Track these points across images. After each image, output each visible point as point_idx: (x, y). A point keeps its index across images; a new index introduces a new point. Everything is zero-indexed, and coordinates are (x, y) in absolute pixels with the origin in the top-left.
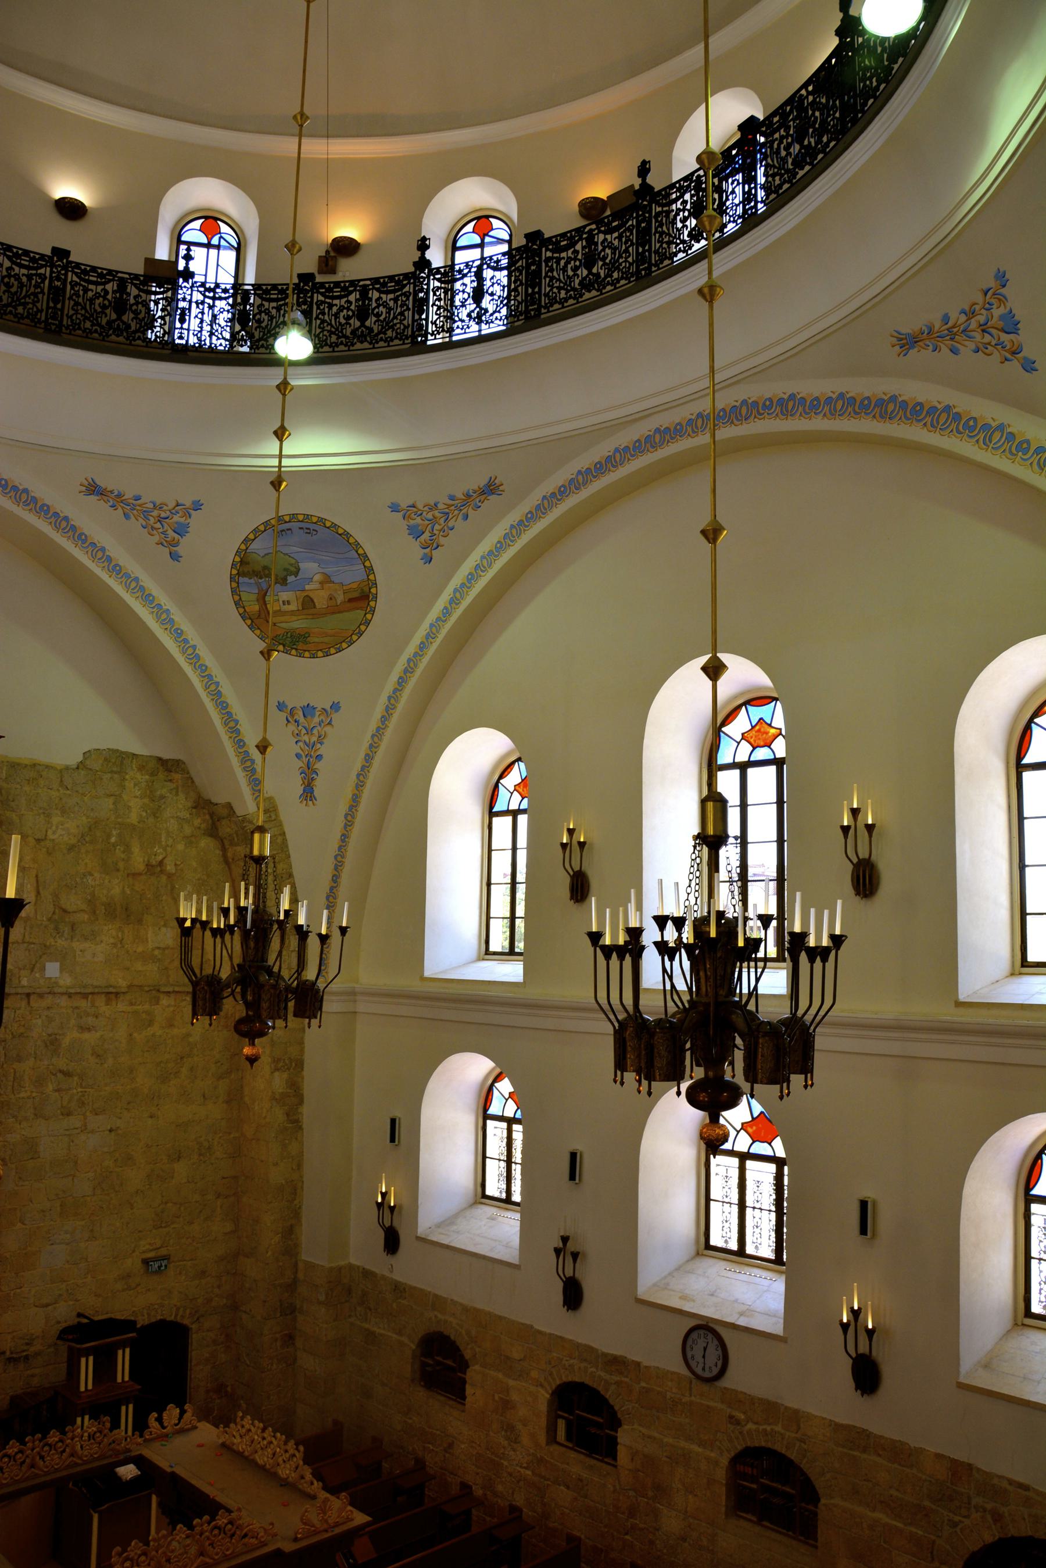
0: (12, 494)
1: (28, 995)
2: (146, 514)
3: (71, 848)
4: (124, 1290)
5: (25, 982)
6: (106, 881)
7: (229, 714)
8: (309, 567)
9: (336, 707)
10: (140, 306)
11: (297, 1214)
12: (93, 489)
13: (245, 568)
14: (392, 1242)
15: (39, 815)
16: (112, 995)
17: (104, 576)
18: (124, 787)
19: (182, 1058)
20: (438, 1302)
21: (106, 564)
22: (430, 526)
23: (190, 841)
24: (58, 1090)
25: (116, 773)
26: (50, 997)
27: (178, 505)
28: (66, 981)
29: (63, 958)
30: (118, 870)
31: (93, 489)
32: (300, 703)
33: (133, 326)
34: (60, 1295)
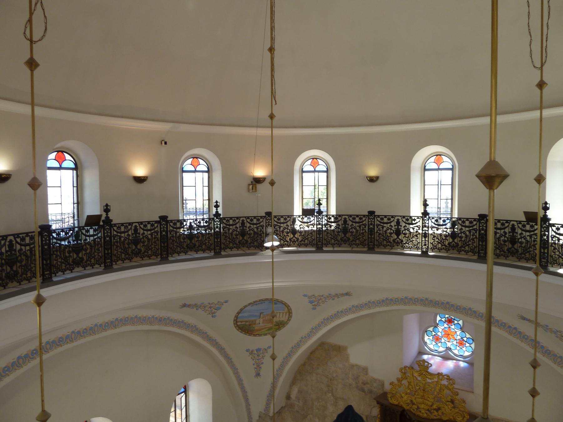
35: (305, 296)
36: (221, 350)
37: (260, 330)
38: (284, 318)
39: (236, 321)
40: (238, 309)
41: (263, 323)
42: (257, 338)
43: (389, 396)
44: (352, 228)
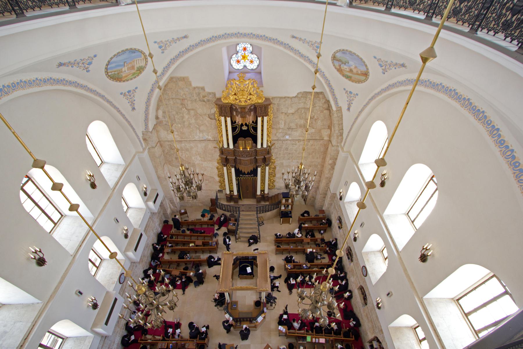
2: (308, 43)
7: (332, 88)
8: (351, 63)
9: (357, 95)
11: (330, 181)
12: (293, 37)
13: (334, 58)
14: (341, 199)
16: (299, 140)
20: (342, 214)
22: (385, 67)
23: (322, 112)
28: (290, 139)
29: (289, 135)
31: (293, 37)
35: (155, 42)
36: (103, 97)
37: (126, 76)
38: (143, 64)
39: (107, 72)
40: (106, 62)
41: (128, 70)
42: (126, 83)
43: (222, 99)
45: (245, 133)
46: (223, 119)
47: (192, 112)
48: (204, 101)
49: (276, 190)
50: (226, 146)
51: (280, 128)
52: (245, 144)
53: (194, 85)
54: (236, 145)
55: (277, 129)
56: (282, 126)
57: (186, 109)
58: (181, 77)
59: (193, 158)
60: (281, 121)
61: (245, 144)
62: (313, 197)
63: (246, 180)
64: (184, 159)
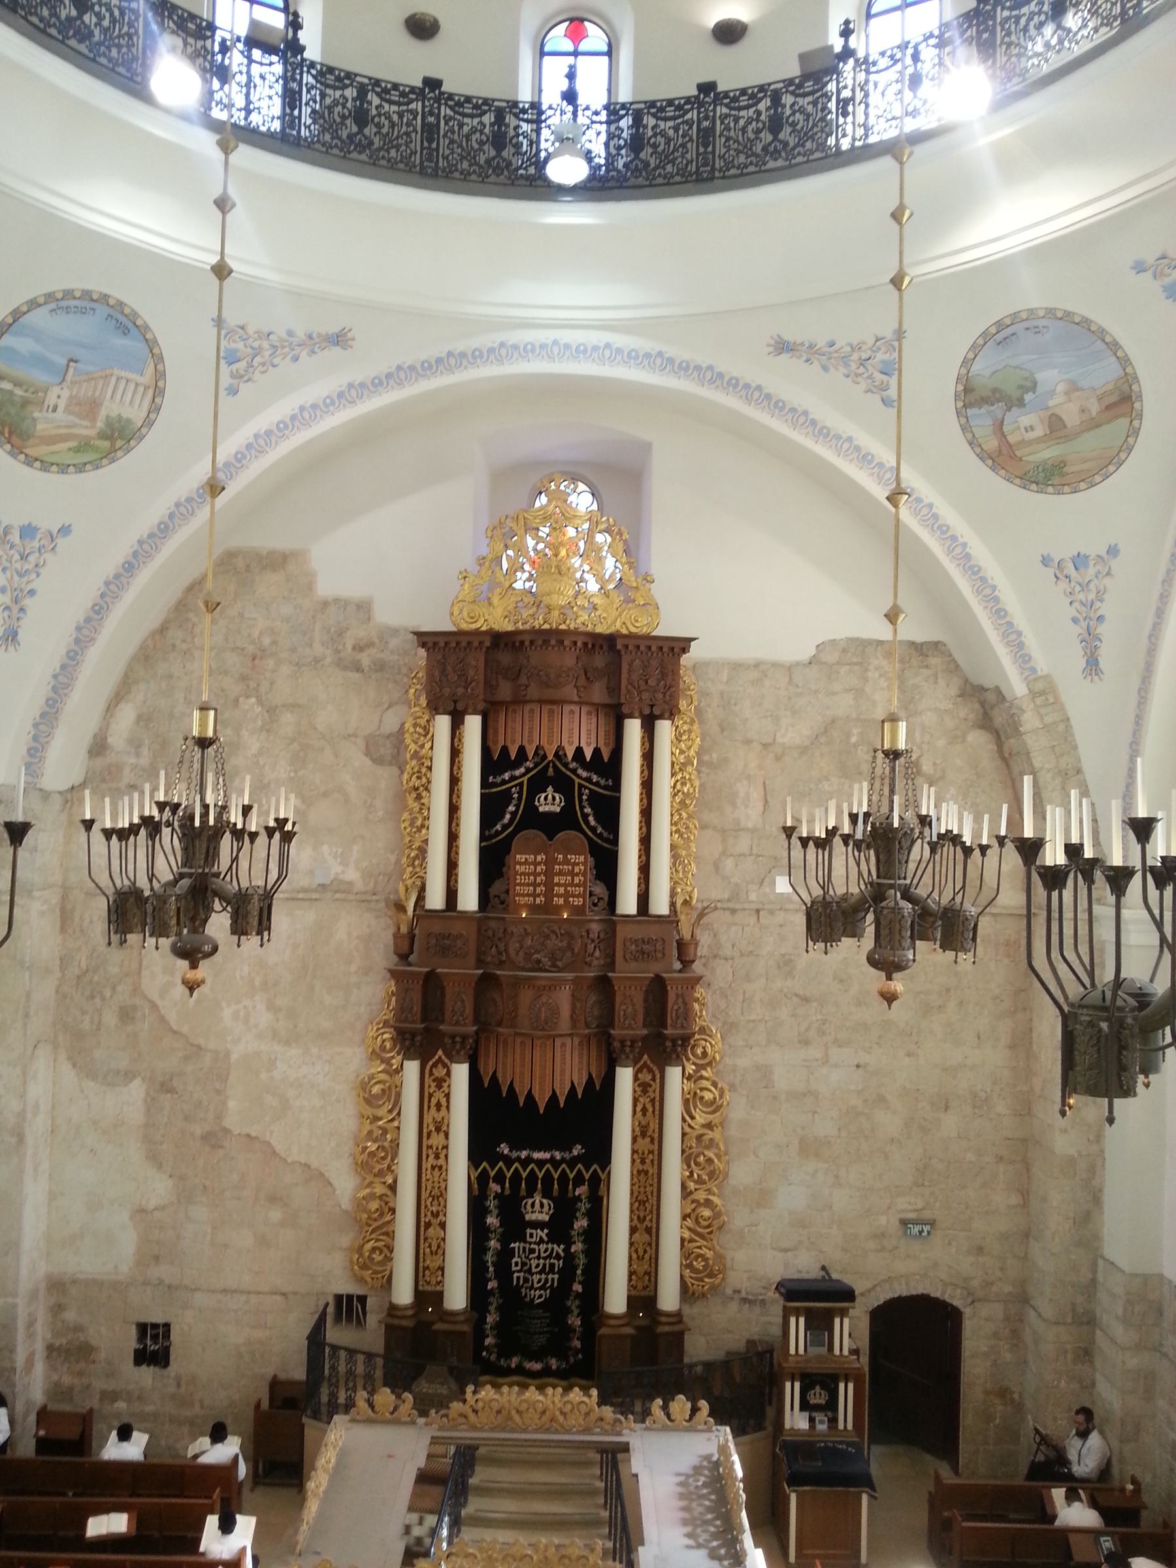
0: (696, 374)
1: (758, 911)
3: (803, 750)
4: (878, 1251)
5: (753, 896)
6: (846, 787)
10: (797, 114)
12: (783, 347)
15: (766, 717)
17: (809, 443)
18: (866, 680)
19: (948, 990)
21: (810, 429)
24: (793, 1015)
25: (856, 664)
26: (782, 914)
27: (877, 340)
30: (860, 773)
31: (783, 347)
32: (1068, 553)
33: (792, 142)
34: (801, 1242)
44: (379, 115)
45: (551, 808)
46: (443, 723)
47: (288, 720)
48: (358, 669)
49: (734, 1306)
50: (436, 899)
51: (738, 829)
52: (549, 874)
53: (325, 588)
54: (497, 888)
55: (723, 831)
56: (750, 814)
57: (260, 702)
58: (271, 553)
59: (227, 1013)
60: (742, 788)
61: (549, 874)
62: (1003, 1393)
63: (540, 1150)
64: (172, 1018)
